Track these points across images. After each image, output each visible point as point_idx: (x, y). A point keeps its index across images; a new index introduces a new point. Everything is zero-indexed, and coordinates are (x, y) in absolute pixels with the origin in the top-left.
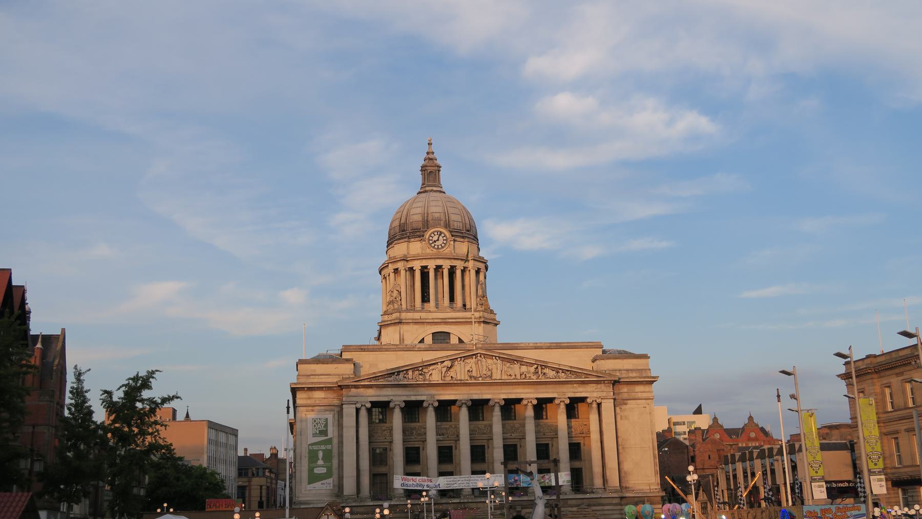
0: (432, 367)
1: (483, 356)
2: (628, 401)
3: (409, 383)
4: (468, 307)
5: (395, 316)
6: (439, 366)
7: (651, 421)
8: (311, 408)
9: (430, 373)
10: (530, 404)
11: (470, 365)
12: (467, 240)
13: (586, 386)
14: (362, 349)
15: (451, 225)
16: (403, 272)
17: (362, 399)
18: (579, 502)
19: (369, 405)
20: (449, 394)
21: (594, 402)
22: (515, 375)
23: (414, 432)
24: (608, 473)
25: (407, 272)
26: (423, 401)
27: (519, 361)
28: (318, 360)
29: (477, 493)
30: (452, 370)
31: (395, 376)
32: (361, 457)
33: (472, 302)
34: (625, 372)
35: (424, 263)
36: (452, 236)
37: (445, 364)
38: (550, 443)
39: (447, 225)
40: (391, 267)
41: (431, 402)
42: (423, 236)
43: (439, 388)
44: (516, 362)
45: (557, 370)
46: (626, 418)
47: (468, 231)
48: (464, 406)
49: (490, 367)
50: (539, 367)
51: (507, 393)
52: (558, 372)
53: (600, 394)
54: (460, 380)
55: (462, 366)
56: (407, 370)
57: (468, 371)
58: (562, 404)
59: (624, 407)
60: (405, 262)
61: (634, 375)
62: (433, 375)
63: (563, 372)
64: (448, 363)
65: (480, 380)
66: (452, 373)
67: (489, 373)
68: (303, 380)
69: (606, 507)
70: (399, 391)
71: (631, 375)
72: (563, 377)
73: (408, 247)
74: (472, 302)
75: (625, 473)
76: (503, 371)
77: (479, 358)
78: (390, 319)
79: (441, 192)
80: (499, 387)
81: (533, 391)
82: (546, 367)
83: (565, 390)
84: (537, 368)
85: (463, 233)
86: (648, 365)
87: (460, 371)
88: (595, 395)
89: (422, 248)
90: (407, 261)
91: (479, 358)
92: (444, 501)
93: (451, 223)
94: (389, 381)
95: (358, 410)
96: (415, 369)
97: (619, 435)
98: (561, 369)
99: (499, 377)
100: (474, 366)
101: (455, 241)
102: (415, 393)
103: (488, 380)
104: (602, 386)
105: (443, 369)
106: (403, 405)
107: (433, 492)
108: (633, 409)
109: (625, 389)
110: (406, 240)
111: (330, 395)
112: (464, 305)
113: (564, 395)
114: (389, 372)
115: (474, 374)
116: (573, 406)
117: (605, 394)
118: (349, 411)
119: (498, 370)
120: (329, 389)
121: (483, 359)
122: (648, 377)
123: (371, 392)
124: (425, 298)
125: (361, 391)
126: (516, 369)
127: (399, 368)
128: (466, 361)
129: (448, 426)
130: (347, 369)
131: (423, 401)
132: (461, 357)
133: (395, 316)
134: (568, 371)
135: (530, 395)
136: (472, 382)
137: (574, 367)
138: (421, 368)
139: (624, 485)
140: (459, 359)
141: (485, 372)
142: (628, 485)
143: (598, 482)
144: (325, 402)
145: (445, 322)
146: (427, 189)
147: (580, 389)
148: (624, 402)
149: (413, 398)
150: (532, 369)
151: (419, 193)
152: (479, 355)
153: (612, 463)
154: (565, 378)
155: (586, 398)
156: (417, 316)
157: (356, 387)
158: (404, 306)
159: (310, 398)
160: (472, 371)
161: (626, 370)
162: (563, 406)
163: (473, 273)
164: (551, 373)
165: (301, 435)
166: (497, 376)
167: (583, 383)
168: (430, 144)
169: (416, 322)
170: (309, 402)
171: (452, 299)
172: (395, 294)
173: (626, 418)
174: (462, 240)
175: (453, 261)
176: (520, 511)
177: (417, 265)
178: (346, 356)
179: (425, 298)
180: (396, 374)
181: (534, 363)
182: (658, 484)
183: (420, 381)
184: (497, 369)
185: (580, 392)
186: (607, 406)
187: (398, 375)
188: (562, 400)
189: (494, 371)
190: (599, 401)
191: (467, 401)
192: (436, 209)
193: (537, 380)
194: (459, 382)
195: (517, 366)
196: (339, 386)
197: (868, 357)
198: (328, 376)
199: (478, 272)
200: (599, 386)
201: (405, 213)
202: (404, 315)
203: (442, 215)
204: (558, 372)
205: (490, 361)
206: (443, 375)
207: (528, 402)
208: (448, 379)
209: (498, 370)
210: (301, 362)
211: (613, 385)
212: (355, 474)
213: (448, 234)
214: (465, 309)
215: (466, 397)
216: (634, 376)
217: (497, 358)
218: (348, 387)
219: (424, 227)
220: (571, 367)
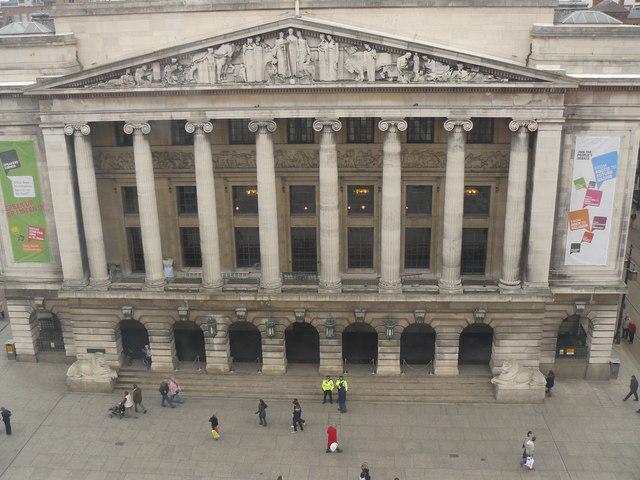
0: (195, 58)
1: (299, 34)
2: (592, 124)
3: (153, 90)
6: (209, 56)
9: (194, 68)
10: (393, 130)
14: (86, 10)
17: (75, 118)
20: (233, 109)
21: (524, 129)
22: (365, 73)
24: (531, 259)
26: (184, 122)
30: (238, 61)
31: (126, 76)
34: (595, 64)
37: (222, 51)
38: (434, 185)
44: (367, 46)
45: (454, 66)
48: (263, 131)
50: (416, 58)
51: (349, 108)
53: (535, 114)
54: (252, 83)
55: (259, 54)
56: (149, 65)
57: (269, 64)
58: (458, 130)
62: (200, 74)
63: (465, 69)
64: (226, 50)
65: (293, 84)
67: (311, 69)
69: (517, 314)
70: (140, 105)
72: (464, 78)
76: (341, 65)
77: (291, 38)
81: (402, 104)
84: (412, 57)
87: (254, 65)
88: (526, 115)
91: (291, 38)
95: (70, 140)
96: (163, 63)
98: (459, 62)
99: (333, 77)
100: (280, 53)
102: (169, 106)
103: (307, 84)
104: (545, 99)
105: (218, 61)
109: (589, 100)
111: (28, 106)
113: (465, 113)
114: (114, 69)
115: (282, 70)
117: (545, 114)
118: (55, 140)
119: (330, 64)
121: (301, 40)
125: (70, 104)
126: (366, 62)
127: (132, 59)
128: (268, 42)
129: (249, 152)
132: (254, 37)
135: (392, 112)
136: (275, 87)
137: (489, 61)
138: (174, 60)
140: (250, 41)
141: (305, 67)
142: (563, 272)
143: (510, 271)
147: (496, 102)
150: (402, 61)
152: (291, 31)
153: (541, 245)
154: (469, 82)
157: (62, 97)
160: (277, 64)
161: (598, 61)
162: (458, 134)
164: (437, 70)
166: (329, 75)
180: (128, 71)
181: (406, 48)
182: (619, 275)
183: (173, 86)
184: (328, 60)
185: (496, 109)
186: (549, 141)
187: (132, 73)
188: (458, 123)
189: (322, 64)
190: (532, 127)
193: (408, 86)
194: (250, 87)
195: (368, 55)
198: (18, 71)
200: (538, 97)
205: (313, 42)
206: (219, 72)
207: (390, 126)
208: (229, 83)
212: (77, 247)
217: (329, 37)
220: (483, 59)
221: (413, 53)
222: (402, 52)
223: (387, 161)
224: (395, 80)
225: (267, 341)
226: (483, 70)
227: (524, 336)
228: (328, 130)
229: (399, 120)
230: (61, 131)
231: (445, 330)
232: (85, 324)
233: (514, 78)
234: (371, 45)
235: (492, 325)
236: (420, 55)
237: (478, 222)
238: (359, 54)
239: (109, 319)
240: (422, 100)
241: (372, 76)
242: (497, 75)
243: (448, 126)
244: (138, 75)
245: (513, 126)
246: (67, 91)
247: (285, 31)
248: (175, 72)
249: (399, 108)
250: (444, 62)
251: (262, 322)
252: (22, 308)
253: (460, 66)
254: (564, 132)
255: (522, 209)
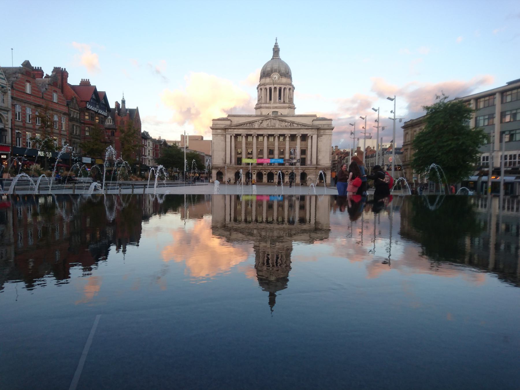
0: (255, 123)
4: (285, 102)
5: (259, 105)
6: (258, 122)
7: (330, 142)
8: (216, 135)
11: (268, 122)
12: (287, 77)
13: (308, 130)
15: (281, 72)
16: (263, 90)
17: (232, 133)
18: (302, 168)
19: (278, 135)
23: (251, 144)
25: (265, 90)
27: (285, 121)
28: (219, 120)
29: (269, 164)
30: (262, 124)
32: (232, 152)
33: (287, 101)
35: (270, 86)
36: (281, 76)
39: (279, 72)
40: (260, 88)
41: (255, 134)
42: (270, 76)
43: (258, 130)
45: (298, 124)
46: (321, 141)
47: (287, 74)
48: (266, 136)
49: (275, 123)
50: (292, 123)
52: (298, 125)
54: (265, 127)
56: (247, 124)
57: (267, 124)
58: (299, 136)
59: (321, 137)
60: (264, 86)
61: (326, 126)
64: (260, 121)
65: (271, 127)
66: (262, 125)
68: (214, 126)
71: (325, 126)
72: (299, 127)
73: (265, 80)
74: (287, 101)
75: (319, 160)
77: (271, 120)
78: (258, 106)
79: (279, 59)
80: (278, 130)
82: (294, 123)
83: (300, 131)
84: (291, 123)
85: (285, 75)
86: (332, 122)
87: (265, 124)
88: (311, 133)
89: (270, 80)
90: (265, 85)
91: (271, 120)
92: (258, 166)
93: (281, 71)
94: (241, 127)
95: (231, 137)
97: (318, 147)
101: (281, 77)
104: (313, 130)
106: (246, 135)
107: (276, 163)
108: (324, 139)
109: (322, 131)
110: (265, 77)
111: (223, 131)
112: (284, 102)
116: (304, 137)
117: (314, 133)
118: (228, 137)
120: (222, 129)
122: (331, 127)
123: (235, 130)
124: (270, 99)
125: (232, 130)
126: (284, 124)
127: (244, 123)
128: (267, 121)
130: (228, 123)
131: (252, 134)
132: (265, 120)
133: (259, 105)
134: (302, 125)
139: (318, 164)
143: (309, 162)
144: (221, 133)
145: (276, 108)
146: (274, 57)
148: (321, 136)
149: (249, 133)
150: (289, 124)
151: (272, 59)
155: (307, 134)
156: (267, 105)
157: (230, 129)
158: (263, 102)
159: (216, 132)
162: (299, 137)
163: (288, 89)
164: (295, 125)
165: (213, 144)
167: (307, 129)
168: (276, 40)
169: (267, 108)
170: (216, 133)
171: (280, 99)
172: (260, 97)
173: (321, 141)
174: (285, 77)
175: (280, 85)
176: (220, 170)
177: (268, 87)
178: (229, 118)
179: (270, 99)
184: (277, 123)
186: (315, 137)
190: (312, 135)
191: (267, 134)
192: (276, 66)
196: (225, 128)
197: (411, 120)
199: (290, 89)
200: (312, 130)
201: (265, 67)
202: (262, 105)
203: (278, 68)
204: (298, 125)
205: (275, 121)
208: (261, 127)
209: (278, 124)
210: (213, 120)
211: (318, 130)
213: (279, 75)
214: (284, 103)
215: (267, 133)
216: (326, 127)
218: (228, 129)
219: (271, 73)
220: (303, 123)
221: (291, 122)
222: (289, 122)
223: (287, 142)
224: (288, 127)
225: (264, 176)
226: (303, 125)
227: (312, 175)
228: (277, 136)
229: (289, 134)
230: (230, 135)
231: (297, 174)
232: (229, 173)
233: (308, 126)
234: (284, 121)
235: (306, 173)
236: (292, 123)
237: (303, 156)
238: (282, 123)
239: (234, 171)
240: (292, 131)
241: (284, 126)
242: (305, 126)
243: (297, 135)
244: (245, 125)
245: (308, 135)
246: (232, 128)
247: (270, 119)
248: (251, 125)
249: (288, 132)
250: (296, 124)
251: (264, 173)
252: (216, 171)
253: (299, 125)
254: (318, 137)
255: (311, 150)
